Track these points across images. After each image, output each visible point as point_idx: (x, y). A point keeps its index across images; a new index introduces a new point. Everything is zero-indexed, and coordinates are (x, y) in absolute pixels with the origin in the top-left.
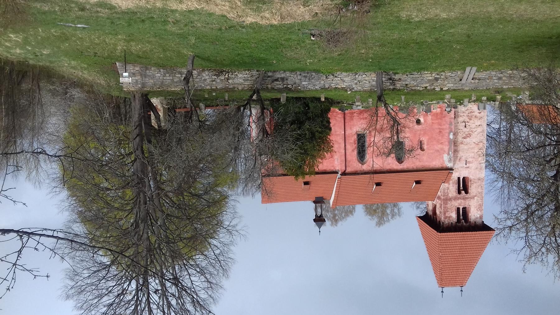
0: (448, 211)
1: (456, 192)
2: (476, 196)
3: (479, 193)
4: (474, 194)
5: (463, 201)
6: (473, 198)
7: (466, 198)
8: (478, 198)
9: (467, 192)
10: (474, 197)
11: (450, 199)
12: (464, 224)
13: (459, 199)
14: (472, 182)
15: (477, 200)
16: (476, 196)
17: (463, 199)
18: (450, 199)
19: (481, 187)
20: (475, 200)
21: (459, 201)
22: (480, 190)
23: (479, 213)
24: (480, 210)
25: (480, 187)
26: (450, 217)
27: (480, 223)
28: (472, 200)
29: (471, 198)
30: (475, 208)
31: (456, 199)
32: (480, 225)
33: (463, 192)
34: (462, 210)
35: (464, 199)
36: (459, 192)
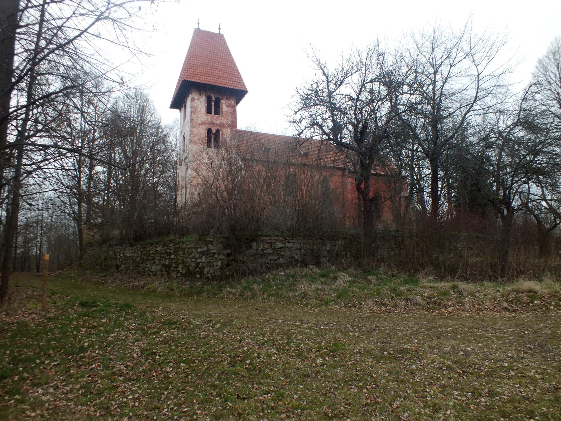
0: (231, 113)
1: (223, 133)
2: (200, 124)
3: (195, 127)
4: (201, 126)
5: (214, 121)
6: (202, 123)
7: (211, 125)
8: (196, 121)
9: (209, 131)
10: (202, 123)
11: (229, 126)
12: (212, 95)
13: (220, 125)
14: (204, 141)
15: (198, 120)
16: (200, 124)
17: (214, 124)
18: (229, 126)
19: (193, 134)
20: (200, 120)
21: (218, 122)
22: (195, 131)
23: (195, 105)
24: (194, 108)
25: (194, 134)
26: (228, 106)
27: (194, 93)
28: (204, 120)
29: (205, 123)
30: (200, 111)
31: (222, 125)
32: (194, 91)
33: (214, 131)
34: (211, 111)
35: (212, 123)
36: (218, 131)
